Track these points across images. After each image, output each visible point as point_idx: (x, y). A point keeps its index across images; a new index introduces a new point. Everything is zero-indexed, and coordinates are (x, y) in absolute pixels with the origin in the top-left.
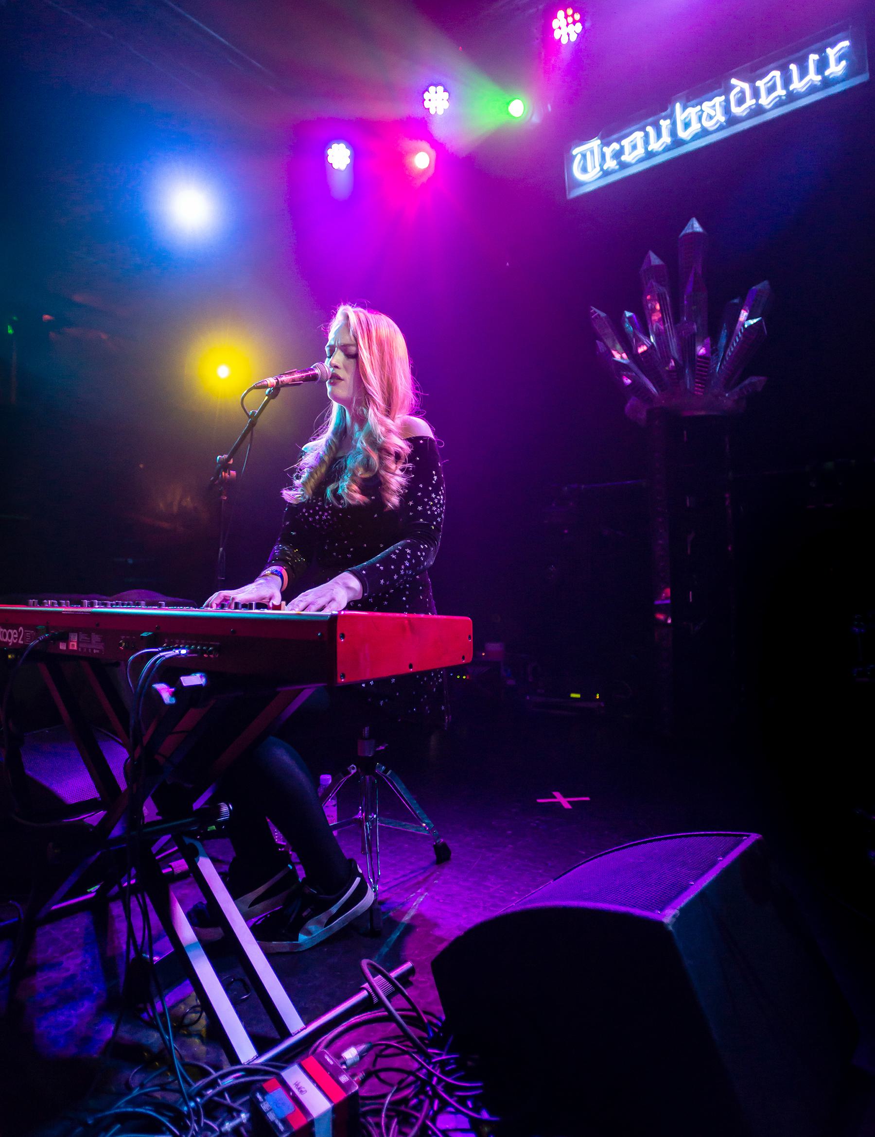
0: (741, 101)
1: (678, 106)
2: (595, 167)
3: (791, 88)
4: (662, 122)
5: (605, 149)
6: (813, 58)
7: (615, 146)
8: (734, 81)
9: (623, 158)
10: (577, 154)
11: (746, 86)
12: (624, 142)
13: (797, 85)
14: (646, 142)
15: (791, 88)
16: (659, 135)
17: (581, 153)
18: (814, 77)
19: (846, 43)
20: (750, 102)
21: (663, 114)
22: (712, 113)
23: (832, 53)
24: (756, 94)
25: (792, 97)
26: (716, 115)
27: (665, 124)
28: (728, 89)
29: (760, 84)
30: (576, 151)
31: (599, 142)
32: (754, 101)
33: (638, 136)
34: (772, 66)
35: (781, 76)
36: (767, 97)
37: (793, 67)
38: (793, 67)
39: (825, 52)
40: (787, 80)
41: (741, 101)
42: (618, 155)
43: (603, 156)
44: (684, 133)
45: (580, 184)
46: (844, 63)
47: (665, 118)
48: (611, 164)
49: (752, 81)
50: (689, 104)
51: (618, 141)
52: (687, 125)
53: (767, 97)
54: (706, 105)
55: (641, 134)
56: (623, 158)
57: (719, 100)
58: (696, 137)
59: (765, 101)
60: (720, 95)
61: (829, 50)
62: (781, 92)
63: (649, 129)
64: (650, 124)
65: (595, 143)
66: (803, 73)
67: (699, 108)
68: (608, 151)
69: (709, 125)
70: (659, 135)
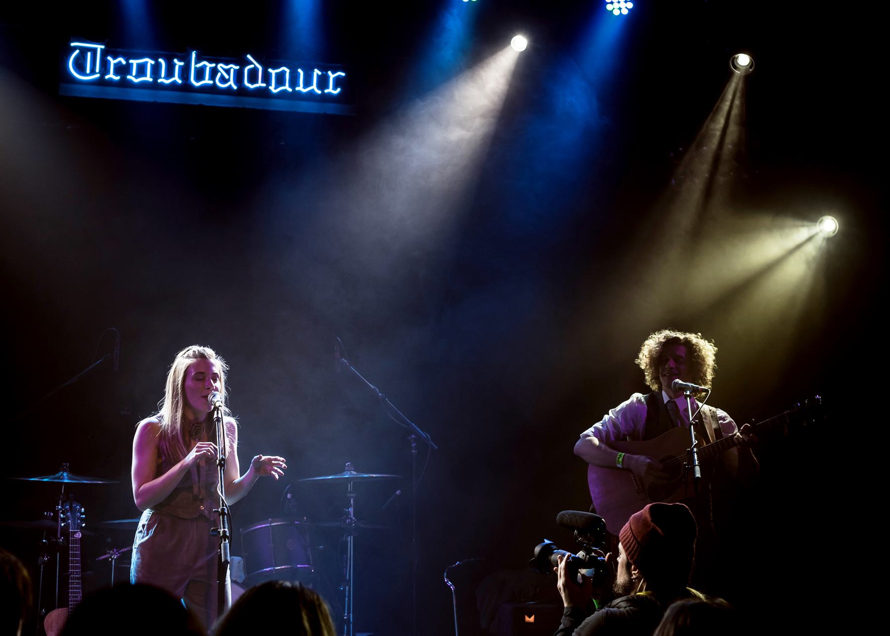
0: (253, 78)
3: (297, 89)
4: (176, 61)
5: (109, 58)
6: (317, 72)
7: (122, 60)
8: (249, 56)
9: (129, 77)
10: (75, 48)
11: (260, 68)
12: (131, 61)
13: (300, 88)
14: (156, 69)
16: (170, 74)
17: (80, 48)
19: (343, 74)
20: (260, 84)
22: (227, 77)
23: (332, 76)
24: (267, 78)
25: (296, 96)
26: (228, 80)
27: (178, 64)
28: (244, 63)
29: (270, 70)
30: (72, 44)
31: (103, 47)
32: (264, 85)
35: (290, 73)
36: (275, 88)
37: (300, 70)
38: (300, 70)
39: (327, 72)
40: (294, 82)
41: (253, 78)
42: (122, 70)
43: (105, 65)
46: (339, 90)
47: (180, 60)
48: (111, 76)
50: (205, 57)
51: (128, 57)
52: (200, 74)
53: (275, 88)
55: (153, 62)
56: (129, 77)
57: (234, 67)
58: (204, 89)
61: (330, 73)
62: (287, 87)
63: (161, 60)
65: (100, 47)
66: (307, 83)
67: (214, 65)
68: (112, 62)
70: (170, 74)
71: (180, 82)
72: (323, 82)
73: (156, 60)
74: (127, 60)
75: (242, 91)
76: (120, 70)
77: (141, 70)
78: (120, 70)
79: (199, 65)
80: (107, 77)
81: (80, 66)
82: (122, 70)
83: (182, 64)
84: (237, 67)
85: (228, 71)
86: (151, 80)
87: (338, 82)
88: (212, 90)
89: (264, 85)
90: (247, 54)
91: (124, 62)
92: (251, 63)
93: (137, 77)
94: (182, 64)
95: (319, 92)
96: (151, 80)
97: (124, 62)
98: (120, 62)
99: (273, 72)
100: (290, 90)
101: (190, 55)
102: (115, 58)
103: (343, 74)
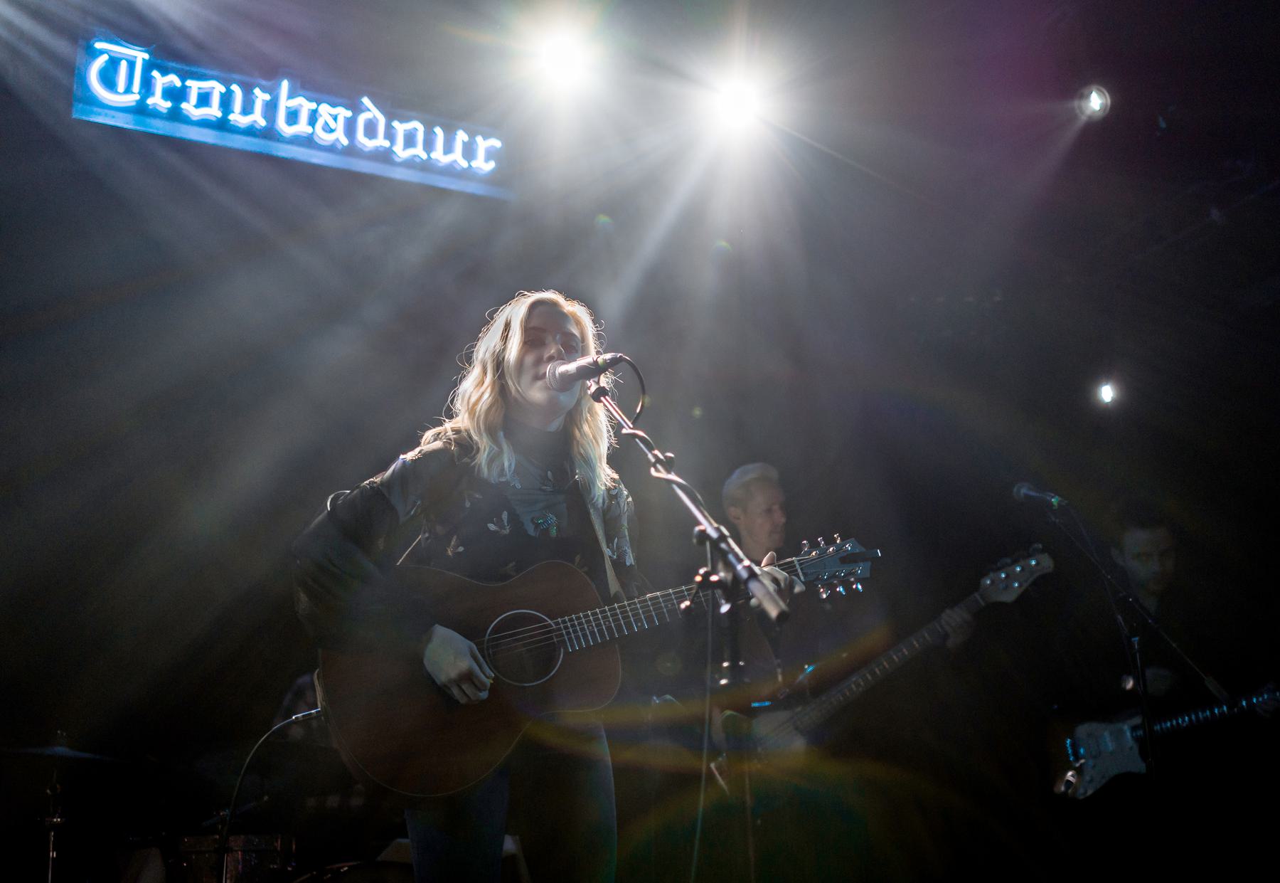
0: (371, 130)
1: (285, 85)
2: (128, 90)
3: (434, 155)
4: (257, 91)
5: (155, 73)
6: (461, 136)
8: (366, 101)
10: (102, 52)
12: (189, 83)
13: (438, 155)
15: (434, 155)
16: (247, 109)
18: (457, 157)
20: (381, 142)
21: (264, 83)
22: (332, 124)
23: (482, 144)
24: (390, 135)
27: (261, 97)
28: (357, 108)
29: (396, 124)
30: (99, 45)
31: (147, 56)
32: (387, 144)
33: (217, 88)
34: (413, 114)
36: (404, 149)
37: (438, 131)
38: (438, 131)
40: (429, 145)
41: (371, 130)
42: (176, 95)
44: (286, 125)
45: (93, 101)
47: (264, 90)
48: (158, 101)
49: (390, 117)
51: (184, 76)
52: (293, 117)
53: (404, 149)
54: (325, 109)
55: (223, 89)
56: (184, 105)
57: (343, 113)
58: (296, 140)
59: (401, 153)
60: (347, 107)
61: (479, 139)
62: (419, 151)
63: (235, 87)
64: (241, 84)
65: (141, 56)
66: (448, 149)
67: (313, 106)
68: (161, 81)
69: (325, 138)
70: (247, 109)
71: (262, 123)
72: (469, 152)
73: (227, 86)
74: (183, 81)
75: (352, 150)
76: (170, 93)
77: (204, 99)
78: (170, 93)
79: (294, 103)
80: (150, 101)
81: (108, 79)
82: (176, 95)
83: (267, 97)
84: (349, 114)
85: (335, 118)
86: (219, 115)
87: (490, 155)
88: (308, 141)
89: (387, 144)
90: (363, 97)
91: (178, 83)
92: (369, 110)
93: (197, 106)
94: (267, 97)
95: (464, 164)
96: (219, 115)
97: (178, 83)
98: (172, 81)
99: (400, 128)
100: (424, 156)
101: (278, 85)
102: (165, 72)
103: (496, 143)
